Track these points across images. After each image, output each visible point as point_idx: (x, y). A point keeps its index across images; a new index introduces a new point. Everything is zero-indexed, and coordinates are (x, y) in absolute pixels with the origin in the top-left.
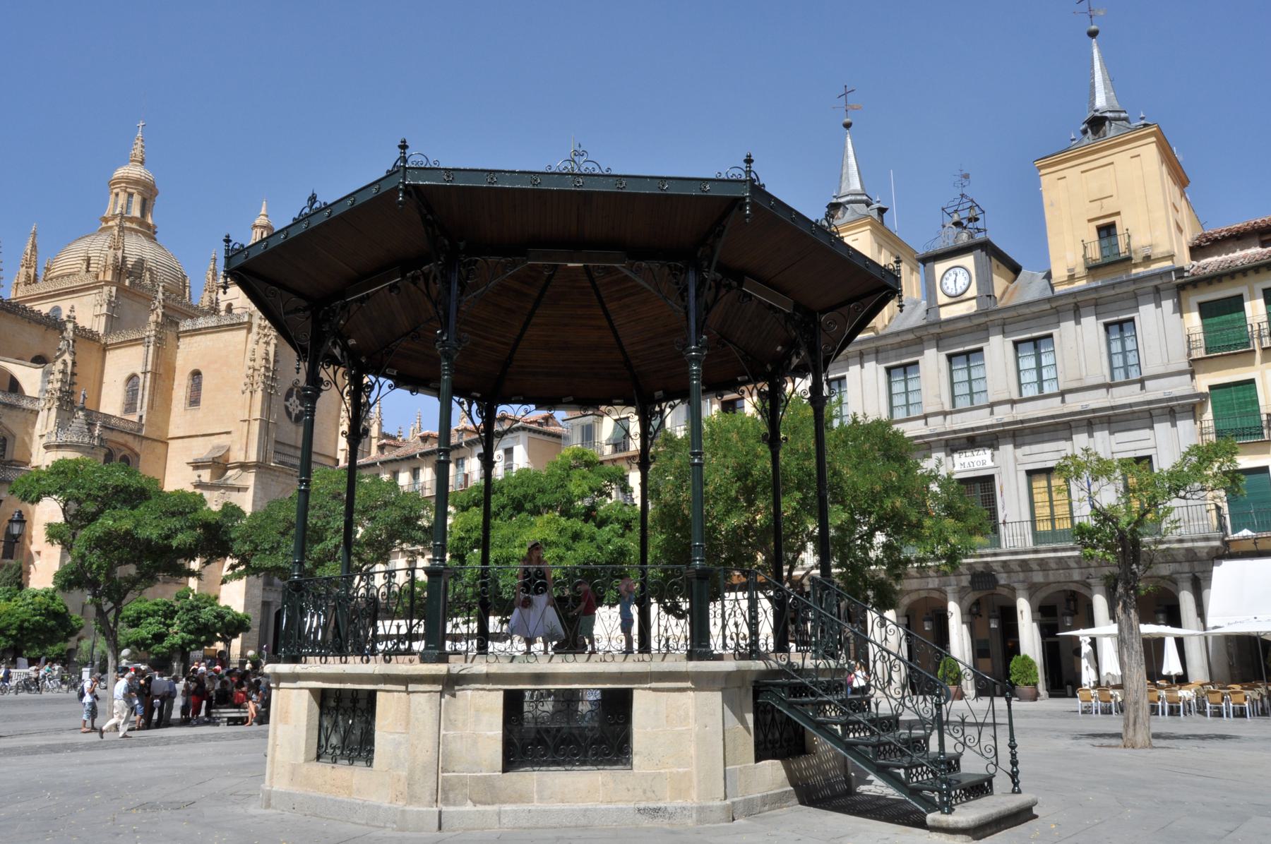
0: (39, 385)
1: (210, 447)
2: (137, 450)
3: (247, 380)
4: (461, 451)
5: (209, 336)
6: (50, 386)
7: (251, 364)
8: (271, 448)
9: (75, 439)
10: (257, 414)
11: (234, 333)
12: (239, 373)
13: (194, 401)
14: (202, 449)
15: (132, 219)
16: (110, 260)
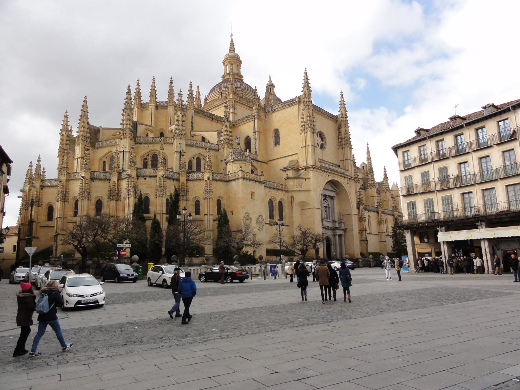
0: (217, 140)
1: (288, 162)
2: (256, 167)
3: (302, 128)
4: (463, 129)
5: (280, 112)
6: (222, 138)
7: (302, 120)
8: (317, 160)
9: (239, 157)
10: (309, 143)
11: (292, 107)
12: (297, 125)
13: (277, 142)
14: (284, 163)
15: (234, 74)
16: (230, 89)
